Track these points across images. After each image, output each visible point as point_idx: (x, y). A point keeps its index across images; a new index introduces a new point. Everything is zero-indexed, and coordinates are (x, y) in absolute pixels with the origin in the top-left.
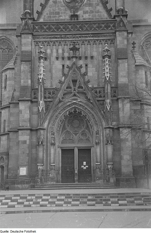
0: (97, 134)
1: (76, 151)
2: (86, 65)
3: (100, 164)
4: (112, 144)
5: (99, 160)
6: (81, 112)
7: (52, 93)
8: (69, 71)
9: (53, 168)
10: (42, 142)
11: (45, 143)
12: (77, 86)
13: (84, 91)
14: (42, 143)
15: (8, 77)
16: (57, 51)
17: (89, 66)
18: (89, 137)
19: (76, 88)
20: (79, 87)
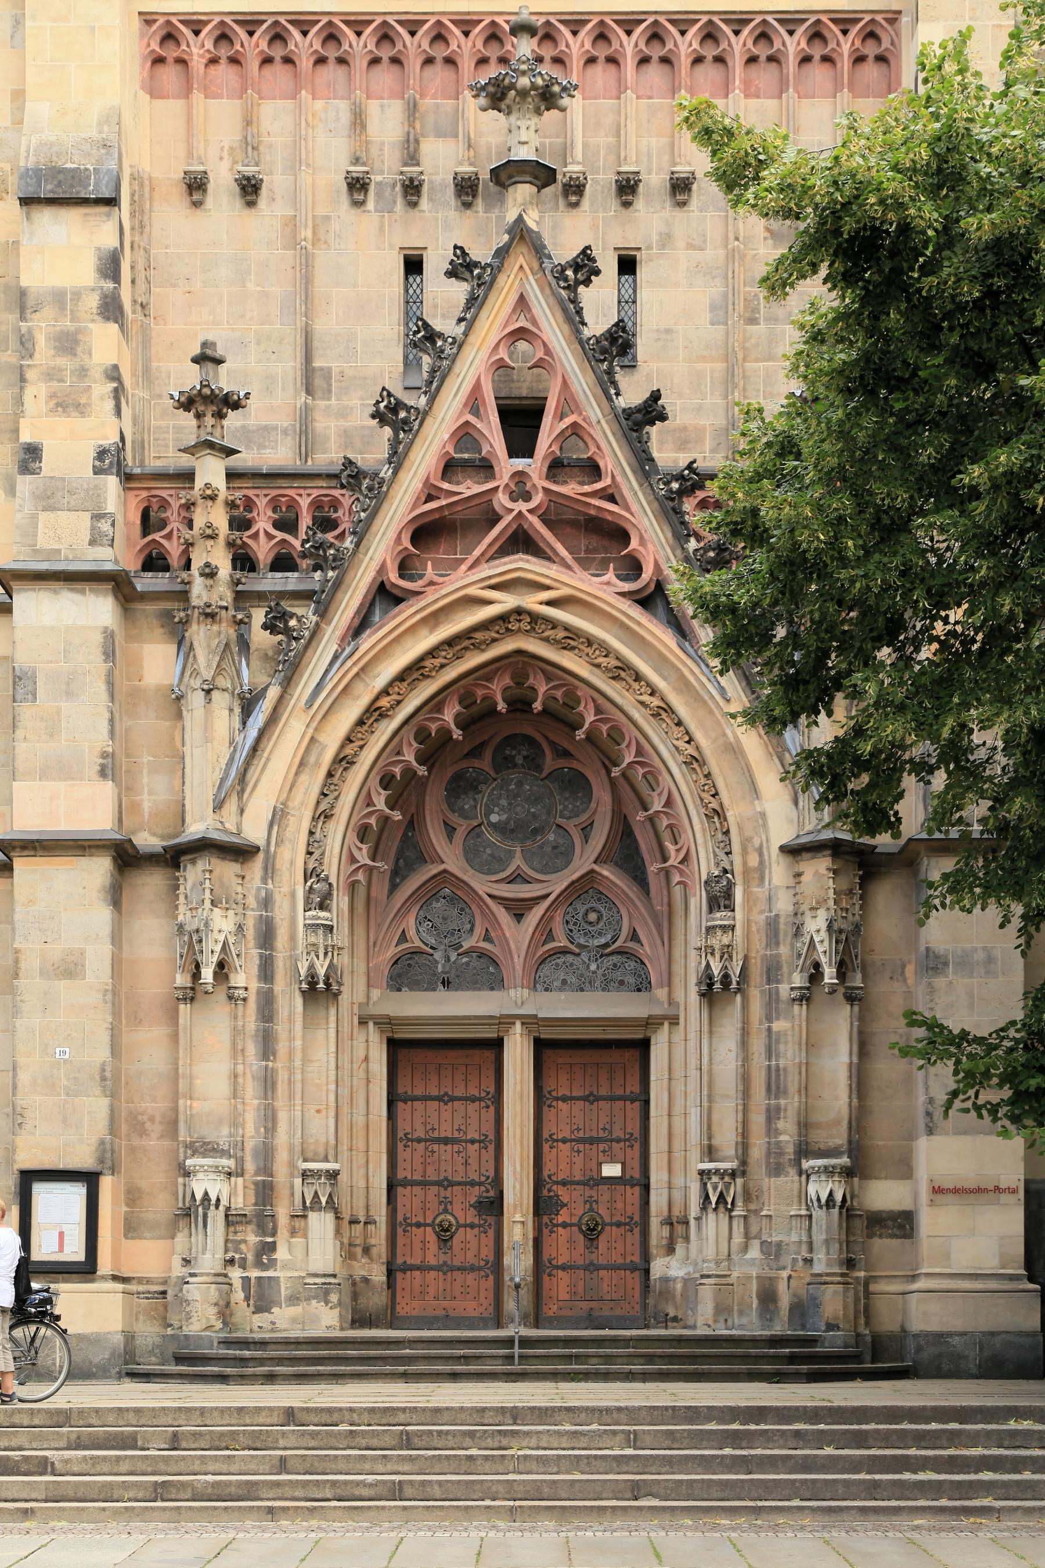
0: (714, 904)
2: (627, 265)
3: (733, 1174)
4: (850, 999)
5: (727, 1138)
6: (572, 700)
7: (305, 522)
8: (474, 302)
9: (324, 1200)
10: (221, 965)
11: (244, 978)
12: (545, 440)
13: (612, 499)
17: (643, 272)
18: (634, 937)
19: (534, 466)
20: (556, 467)
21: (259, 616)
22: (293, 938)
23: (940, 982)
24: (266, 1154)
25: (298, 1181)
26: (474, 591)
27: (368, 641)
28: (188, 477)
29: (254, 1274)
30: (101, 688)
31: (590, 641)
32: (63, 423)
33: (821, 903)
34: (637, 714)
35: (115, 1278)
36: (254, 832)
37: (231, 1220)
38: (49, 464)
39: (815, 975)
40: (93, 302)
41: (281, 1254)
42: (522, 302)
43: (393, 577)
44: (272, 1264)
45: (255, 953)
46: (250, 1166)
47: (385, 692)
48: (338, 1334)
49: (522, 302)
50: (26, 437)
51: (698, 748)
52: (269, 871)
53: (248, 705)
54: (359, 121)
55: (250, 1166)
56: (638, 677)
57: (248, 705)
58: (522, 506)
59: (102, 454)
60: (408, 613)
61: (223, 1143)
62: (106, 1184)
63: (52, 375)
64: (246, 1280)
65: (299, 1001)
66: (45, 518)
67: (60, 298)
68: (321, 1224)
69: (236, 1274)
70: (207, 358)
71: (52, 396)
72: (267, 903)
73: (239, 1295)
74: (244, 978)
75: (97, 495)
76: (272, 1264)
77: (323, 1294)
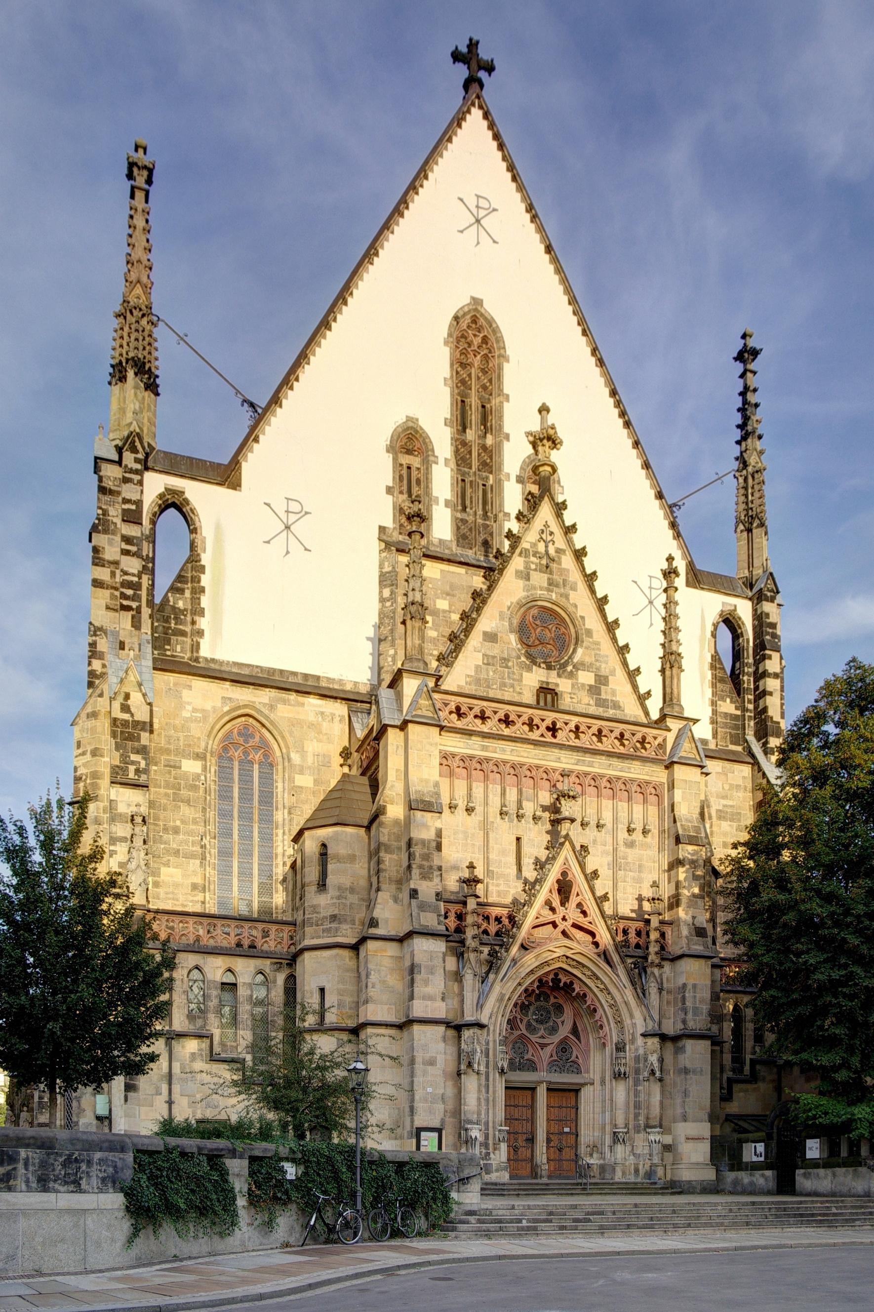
16: (503, 793)
21: (486, 950)
22: (495, 1055)
23: (688, 1077)
24: (487, 1124)
25: (497, 1133)
26: (551, 948)
31: (584, 966)
33: (654, 1052)
34: (595, 990)
36: (484, 1020)
39: (653, 1072)
41: (492, 1155)
42: (566, 859)
44: (490, 1159)
51: (615, 1001)
54: (503, 793)
56: (598, 978)
58: (565, 923)
61: (475, 1120)
65: (497, 1075)
68: (504, 1147)
71: (420, 874)
72: (488, 1044)
76: (490, 1159)
77: (505, 1169)
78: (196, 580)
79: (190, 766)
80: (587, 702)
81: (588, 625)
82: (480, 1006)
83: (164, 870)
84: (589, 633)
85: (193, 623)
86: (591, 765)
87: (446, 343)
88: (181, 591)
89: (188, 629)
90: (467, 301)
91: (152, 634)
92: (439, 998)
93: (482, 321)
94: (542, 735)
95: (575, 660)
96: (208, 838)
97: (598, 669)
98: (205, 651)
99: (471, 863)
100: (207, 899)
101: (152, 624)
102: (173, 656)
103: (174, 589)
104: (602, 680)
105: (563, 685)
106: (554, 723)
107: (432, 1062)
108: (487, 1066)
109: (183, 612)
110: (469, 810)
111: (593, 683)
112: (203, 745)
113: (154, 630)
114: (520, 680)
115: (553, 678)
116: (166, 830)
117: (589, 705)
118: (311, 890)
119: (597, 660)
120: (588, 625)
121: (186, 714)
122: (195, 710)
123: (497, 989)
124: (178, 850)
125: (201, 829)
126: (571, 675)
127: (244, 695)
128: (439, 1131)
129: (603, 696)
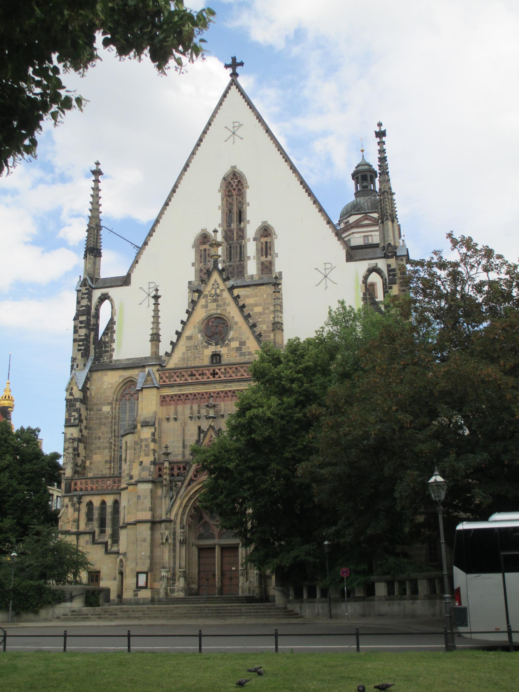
1: (217, 550)
3: (244, 570)
8: (204, 437)
11: (170, 541)
14: (167, 540)
15: (128, 445)
24: (174, 568)
27: (189, 488)
28: (163, 464)
29: (172, 588)
30: (149, 497)
32: (146, 458)
35: (150, 589)
36: (172, 518)
37: (168, 579)
38: (143, 464)
40: (150, 440)
41: (176, 584)
43: (193, 478)
45: (172, 537)
46: (171, 570)
47: (192, 495)
48: (184, 597)
49: (211, 436)
50: (141, 460)
52: (175, 523)
53: (171, 499)
55: (171, 570)
57: (171, 499)
59: (151, 462)
60: (195, 483)
62: (149, 574)
63: (145, 451)
64: (170, 589)
66: (143, 473)
67: (146, 440)
68: (182, 580)
69: (169, 588)
70: (166, 447)
72: (174, 528)
73: (169, 591)
74: (170, 541)
75: (150, 468)
77: (182, 591)
78: (113, 328)
79: (106, 409)
80: (235, 355)
81: (236, 319)
82: (170, 511)
83: (94, 456)
84: (236, 323)
85: (111, 346)
86: (231, 387)
87: (219, 191)
88: (107, 334)
89: (109, 349)
90: (229, 168)
91: (95, 356)
92: (148, 510)
93: (237, 175)
94: (208, 378)
95: (229, 338)
96: (113, 438)
97: (241, 339)
98: (116, 356)
99: (167, 445)
100: (112, 466)
101: (95, 351)
102: (103, 362)
103: (105, 334)
104: (243, 343)
105: (223, 351)
106: (214, 371)
107: (144, 540)
108: (174, 539)
109: (107, 343)
110: (176, 419)
111: (238, 346)
112: (111, 398)
113: (95, 353)
114: (203, 354)
115: (219, 349)
116: (95, 439)
117: (236, 357)
118: (123, 462)
119: (240, 335)
120: (236, 319)
121: (105, 387)
122: (108, 384)
123: (178, 502)
124: (100, 447)
125: (110, 435)
126: (227, 345)
127: (127, 374)
128: (146, 573)
129: (243, 351)
